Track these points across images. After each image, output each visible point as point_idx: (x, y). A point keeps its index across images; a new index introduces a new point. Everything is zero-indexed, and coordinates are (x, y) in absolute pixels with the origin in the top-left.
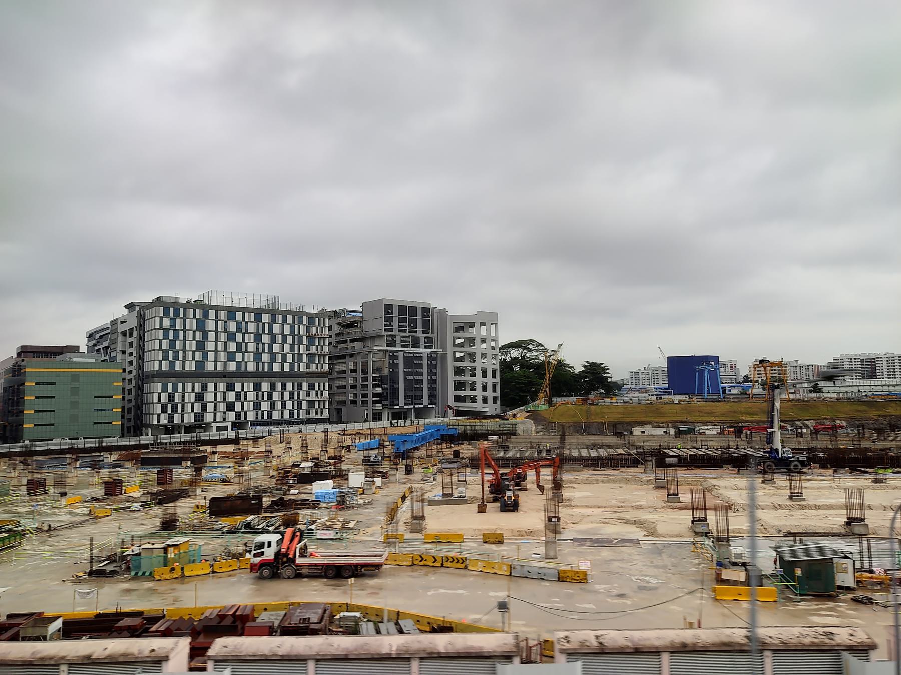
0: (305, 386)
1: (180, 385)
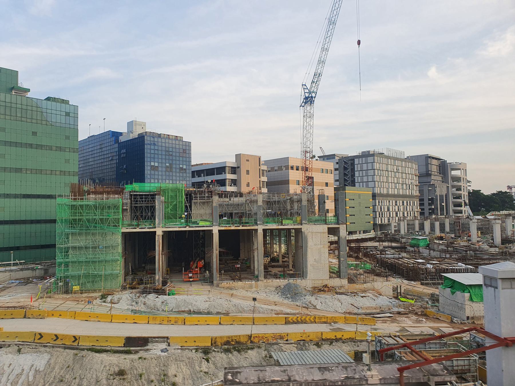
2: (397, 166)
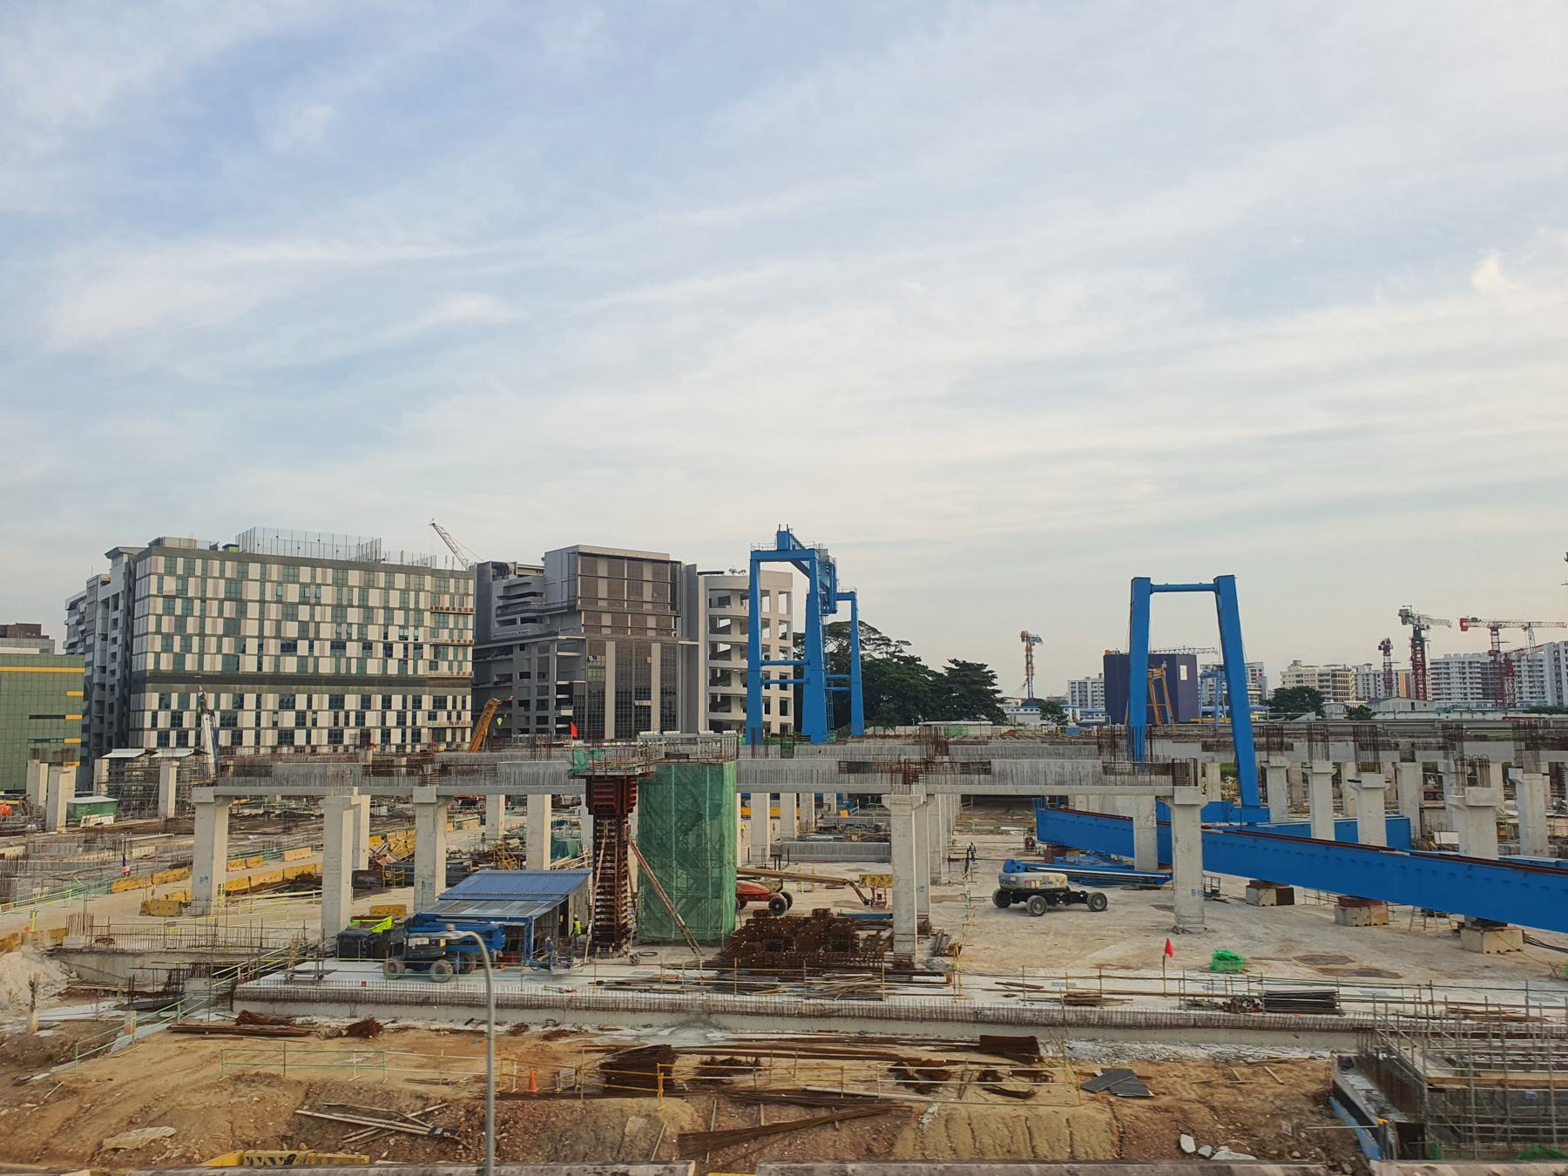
0: (427, 702)
1: (193, 697)
2: (304, 586)
